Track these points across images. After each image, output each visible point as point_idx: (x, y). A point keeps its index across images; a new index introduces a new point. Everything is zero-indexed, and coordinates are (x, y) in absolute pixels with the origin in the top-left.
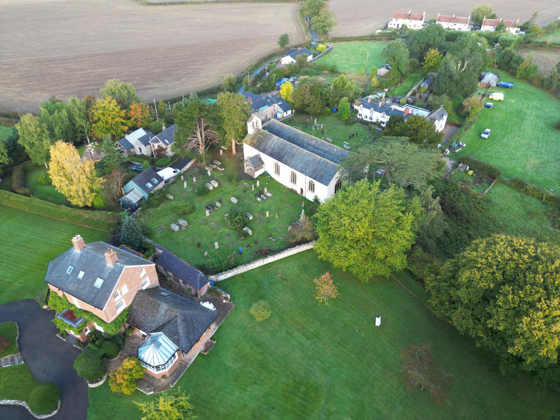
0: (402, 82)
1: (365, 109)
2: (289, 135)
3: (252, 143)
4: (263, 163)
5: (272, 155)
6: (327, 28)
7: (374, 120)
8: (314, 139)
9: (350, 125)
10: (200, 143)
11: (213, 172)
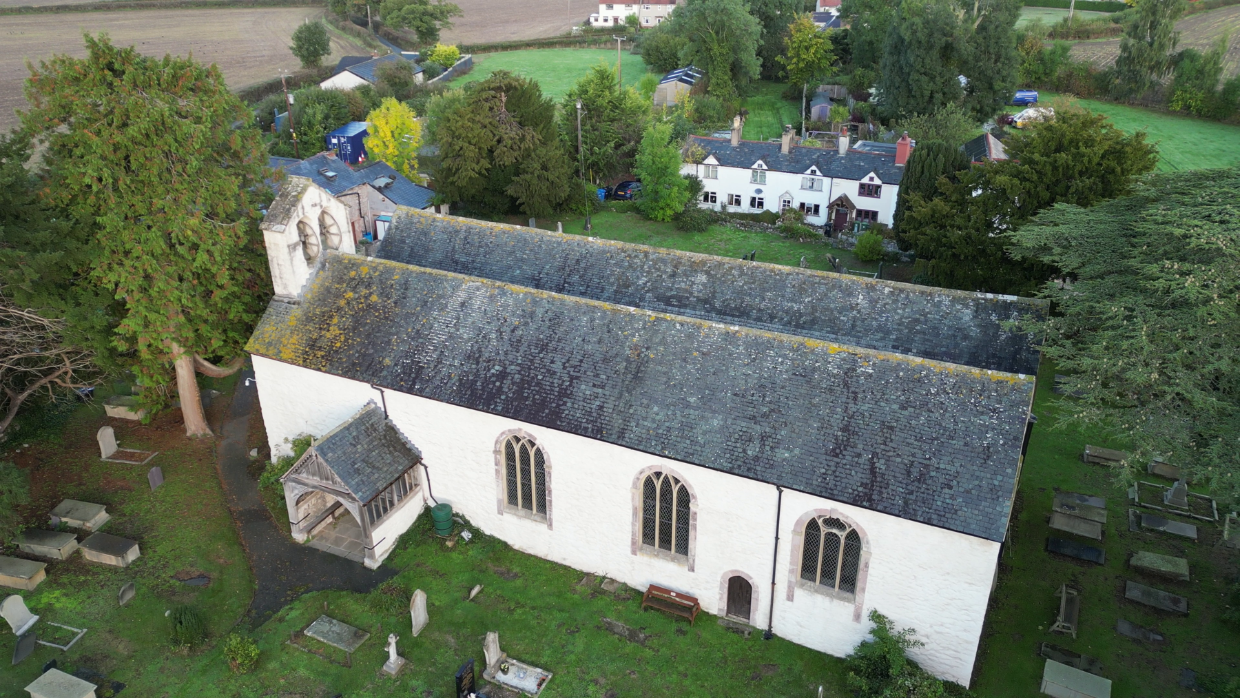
1: (723, 170)
3: (313, 344)
4: (414, 459)
5: (475, 395)
6: (437, 24)
7: (772, 205)
8: (694, 267)
9: (701, 230)
11: (52, 597)
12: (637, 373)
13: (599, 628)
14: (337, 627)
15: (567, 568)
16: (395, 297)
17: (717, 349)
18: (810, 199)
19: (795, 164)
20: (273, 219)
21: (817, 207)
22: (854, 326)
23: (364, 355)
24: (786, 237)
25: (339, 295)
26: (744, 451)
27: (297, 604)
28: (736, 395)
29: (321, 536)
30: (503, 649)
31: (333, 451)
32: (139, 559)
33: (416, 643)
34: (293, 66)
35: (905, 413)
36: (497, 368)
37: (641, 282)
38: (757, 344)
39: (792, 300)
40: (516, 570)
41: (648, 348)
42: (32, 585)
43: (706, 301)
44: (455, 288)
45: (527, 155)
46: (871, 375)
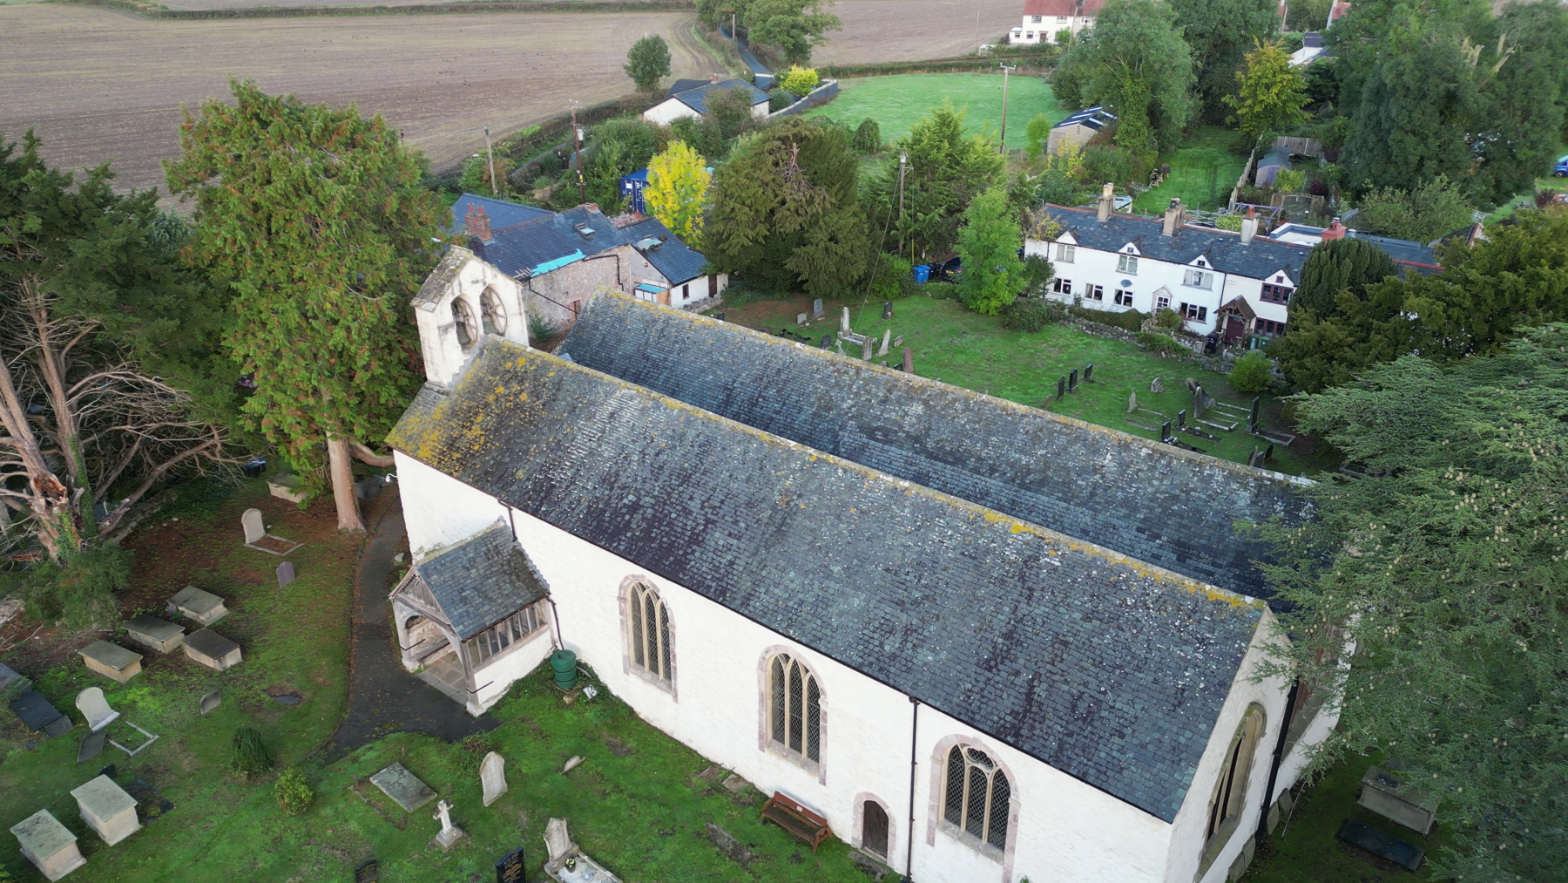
0: (1167, 170)
1: (1082, 254)
2: (724, 377)
3: (452, 444)
4: (540, 592)
5: (600, 529)
6: (808, 38)
7: (1143, 303)
8: (912, 394)
9: (1032, 330)
10: (33, 467)
11: (138, 694)
12: (781, 527)
13: (699, 835)
14: (407, 780)
15: (692, 752)
16: (545, 398)
17: (879, 508)
18: (1195, 298)
19: (1178, 251)
20: (426, 295)
21: (1203, 310)
22: (1092, 494)
23: (498, 463)
24: (1144, 350)
25: (489, 390)
26: (881, 645)
27: (378, 745)
28: (887, 570)
29: (435, 668)
30: (574, 839)
31: (440, 573)
32: (239, 665)
33: (484, 815)
34: (627, 88)
35: (1088, 625)
36: (631, 497)
37: (845, 406)
38: (929, 508)
39: (1021, 451)
40: (632, 744)
41: (800, 496)
42: (122, 678)
43: (917, 439)
44: (608, 395)
45: (814, 221)
46: (1055, 569)
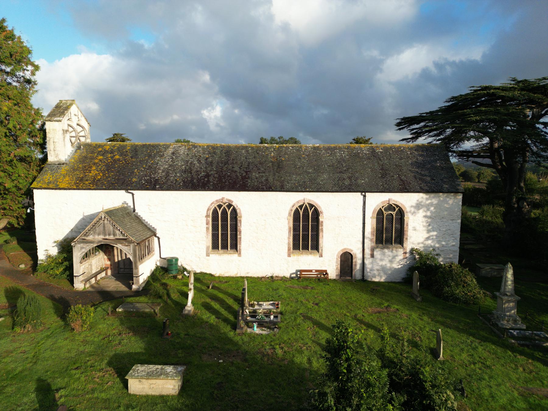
17: (313, 153)
25: (92, 158)
36: (203, 173)
41: (280, 157)
